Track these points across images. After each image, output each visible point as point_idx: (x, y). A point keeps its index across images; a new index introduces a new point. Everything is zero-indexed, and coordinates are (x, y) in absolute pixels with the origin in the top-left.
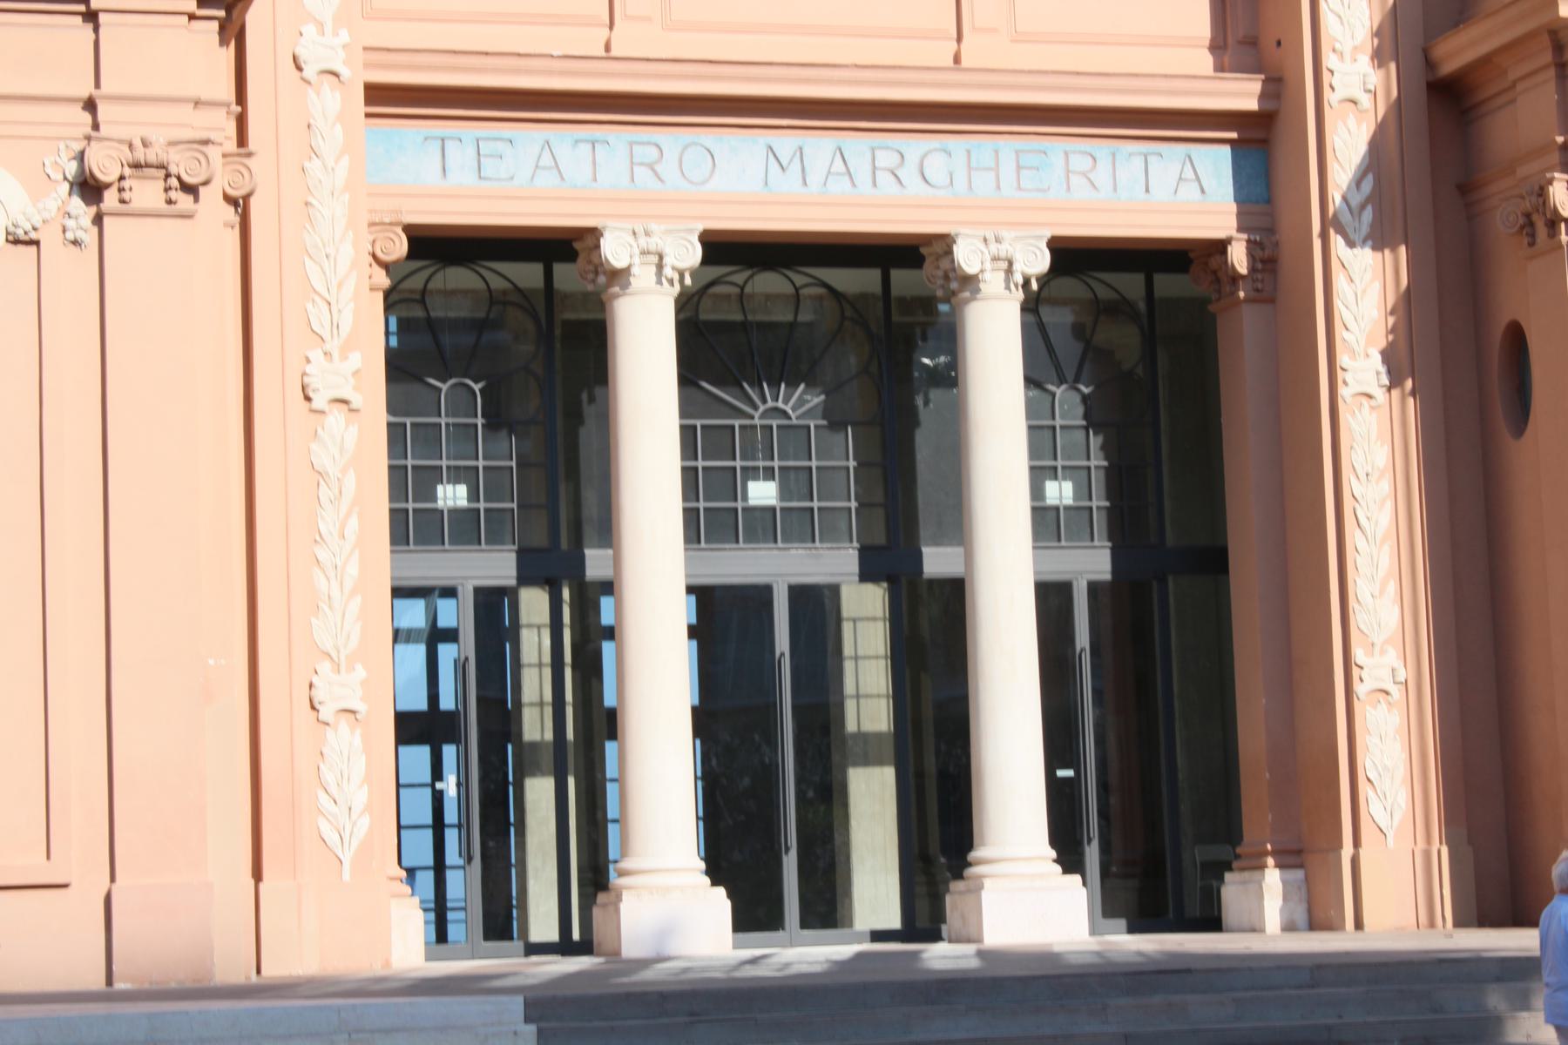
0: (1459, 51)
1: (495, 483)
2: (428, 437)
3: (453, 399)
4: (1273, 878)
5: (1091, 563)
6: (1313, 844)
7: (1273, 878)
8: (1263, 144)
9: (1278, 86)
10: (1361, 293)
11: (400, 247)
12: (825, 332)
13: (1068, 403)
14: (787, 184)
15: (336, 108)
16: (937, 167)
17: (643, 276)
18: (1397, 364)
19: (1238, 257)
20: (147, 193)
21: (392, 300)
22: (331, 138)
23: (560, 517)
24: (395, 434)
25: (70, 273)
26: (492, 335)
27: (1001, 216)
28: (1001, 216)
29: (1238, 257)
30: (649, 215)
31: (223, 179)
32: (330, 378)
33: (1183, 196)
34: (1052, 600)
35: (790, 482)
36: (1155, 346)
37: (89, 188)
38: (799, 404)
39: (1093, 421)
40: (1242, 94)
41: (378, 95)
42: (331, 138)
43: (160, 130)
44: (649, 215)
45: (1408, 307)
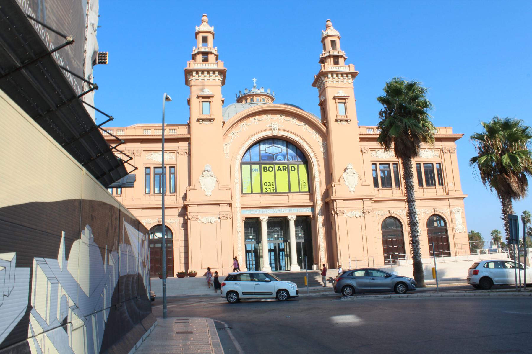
0: (327, 200)
1: (253, 236)
2: (248, 233)
3: (251, 230)
4: (315, 265)
5: (302, 240)
6: (317, 264)
7: (315, 265)
8: (313, 207)
9: (314, 203)
10: (320, 219)
11: (245, 219)
12: (279, 224)
13: (300, 228)
14: (275, 212)
15: (239, 209)
16: (287, 211)
17: (264, 220)
18: (323, 225)
19: (311, 216)
20: (224, 218)
21: (245, 223)
22: (239, 212)
23: (258, 240)
24: (245, 233)
25: (218, 224)
26: (252, 225)
27: (292, 215)
28: (292, 215)
29: (311, 216)
30: (264, 216)
31: (229, 216)
32: (239, 230)
33: (307, 212)
34: (298, 244)
35: (278, 235)
36: (305, 223)
37: (220, 218)
38: (278, 229)
39: (302, 229)
40: (311, 204)
41: (242, 208)
42: (239, 212)
43: (224, 214)
44: (264, 216)
45: (324, 220)
